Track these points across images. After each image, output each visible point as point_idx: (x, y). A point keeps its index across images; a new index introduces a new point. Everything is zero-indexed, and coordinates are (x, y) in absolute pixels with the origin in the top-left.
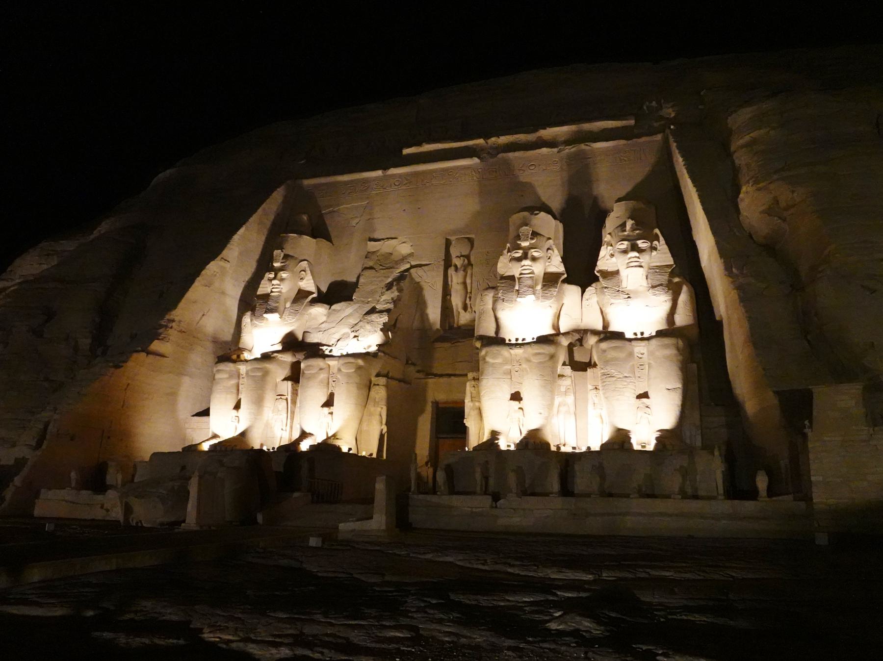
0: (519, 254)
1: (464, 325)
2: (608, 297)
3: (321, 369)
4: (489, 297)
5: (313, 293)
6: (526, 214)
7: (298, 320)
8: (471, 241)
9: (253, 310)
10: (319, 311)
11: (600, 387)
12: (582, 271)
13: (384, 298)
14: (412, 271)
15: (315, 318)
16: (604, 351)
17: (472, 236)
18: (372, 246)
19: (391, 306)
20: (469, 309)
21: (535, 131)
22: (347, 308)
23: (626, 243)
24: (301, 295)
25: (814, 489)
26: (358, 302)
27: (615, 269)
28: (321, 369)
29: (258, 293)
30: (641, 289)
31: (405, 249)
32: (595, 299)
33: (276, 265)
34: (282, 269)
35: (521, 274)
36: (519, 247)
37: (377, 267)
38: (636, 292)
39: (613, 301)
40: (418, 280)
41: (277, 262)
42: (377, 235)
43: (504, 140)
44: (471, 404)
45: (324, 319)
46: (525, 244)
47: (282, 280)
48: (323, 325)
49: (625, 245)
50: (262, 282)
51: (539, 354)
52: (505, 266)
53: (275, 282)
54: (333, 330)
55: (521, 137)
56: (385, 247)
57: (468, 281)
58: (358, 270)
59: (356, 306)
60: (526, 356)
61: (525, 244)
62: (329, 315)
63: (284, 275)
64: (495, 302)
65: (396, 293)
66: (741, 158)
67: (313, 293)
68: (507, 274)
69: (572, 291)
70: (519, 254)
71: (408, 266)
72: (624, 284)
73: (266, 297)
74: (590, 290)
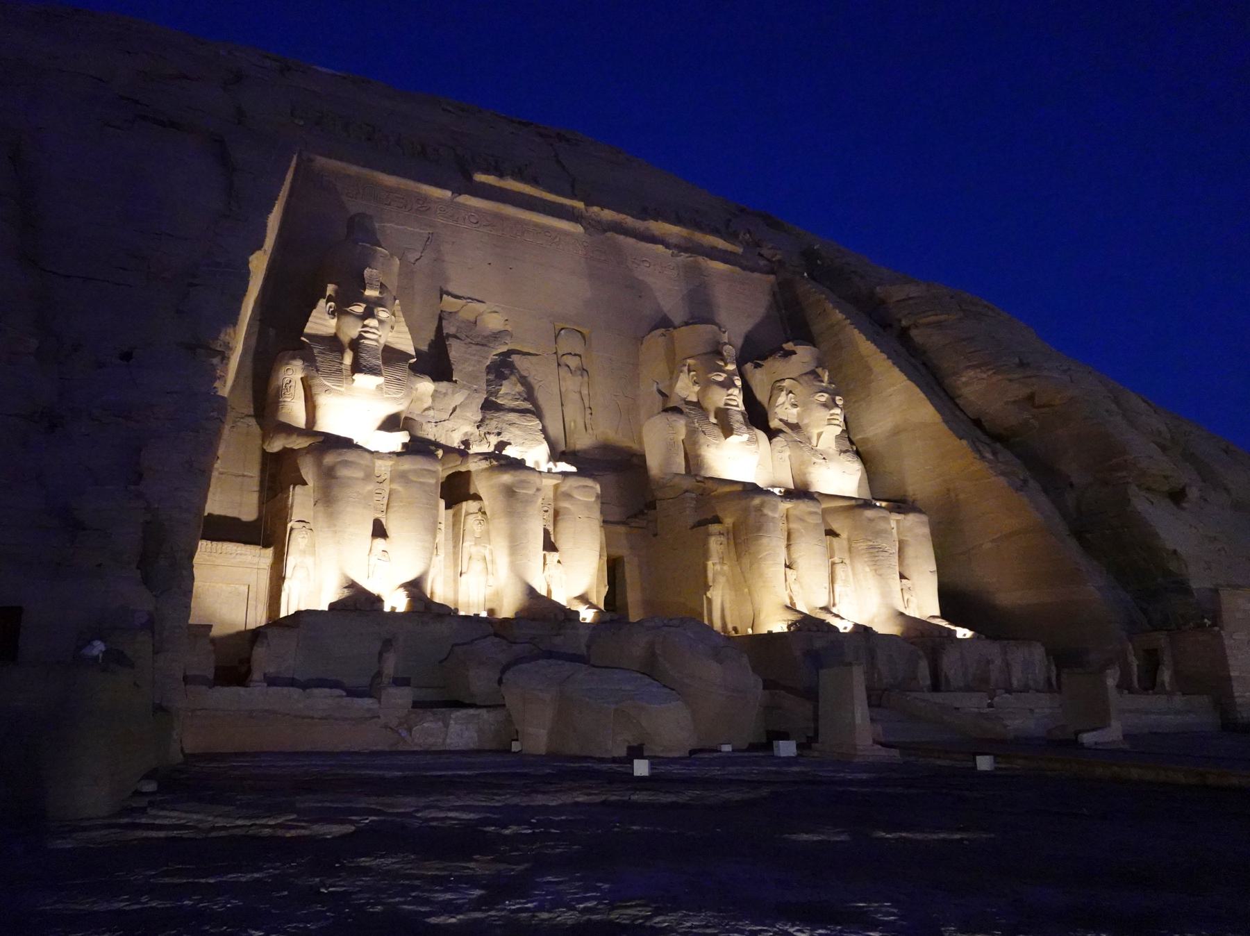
1: (585, 451)
2: (807, 454)
3: (538, 490)
4: (680, 427)
5: (412, 357)
7: (407, 395)
9: (310, 361)
10: (426, 386)
11: (847, 561)
12: (757, 417)
13: (503, 390)
14: (515, 358)
15: (419, 399)
16: (871, 520)
17: (584, 331)
19: (529, 406)
20: (590, 431)
22: (453, 393)
23: (826, 395)
24: (391, 356)
25: (1235, 684)
26: (463, 387)
27: (795, 421)
28: (538, 490)
29: (307, 330)
30: (831, 451)
31: (494, 322)
32: (787, 453)
33: (368, 293)
34: (379, 302)
35: (727, 404)
37: (463, 337)
38: (828, 454)
39: (814, 460)
40: (525, 374)
41: (372, 288)
42: (450, 290)
44: (718, 567)
45: (428, 402)
47: (381, 322)
48: (431, 413)
49: (824, 397)
50: (314, 313)
51: (816, 513)
52: (686, 388)
53: (372, 322)
54: (448, 425)
56: (468, 311)
57: (585, 392)
58: (429, 335)
59: (466, 392)
60: (796, 512)
62: (435, 395)
63: (383, 314)
64: (692, 433)
65: (520, 388)
67: (412, 357)
68: (689, 399)
69: (762, 435)
71: (504, 349)
72: (814, 442)
73: (333, 344)
74: (779, 440)
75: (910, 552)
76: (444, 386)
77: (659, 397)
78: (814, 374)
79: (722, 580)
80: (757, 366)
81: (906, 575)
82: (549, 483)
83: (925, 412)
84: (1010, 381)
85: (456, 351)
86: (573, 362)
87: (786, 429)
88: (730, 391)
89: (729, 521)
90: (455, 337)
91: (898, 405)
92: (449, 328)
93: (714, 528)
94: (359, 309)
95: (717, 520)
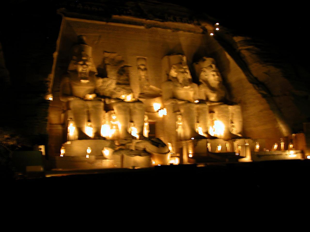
0: (182, 70)
6: (180, 56)
8: (145, 59)
12: (196, 80)
18: (107, 55)
21: (162, 21)
33: (84, 58)
34: (86, 61)
36: (182, 68)
43: (153, 22)
46: (185, 67)
52: (173, 73)
55: (159, 23)
61: (185, 67)
63: (88, 63)
66: (245, 53)
69: (195, 85)
70: (182, 70)
71: (122, 65)
75: (235, 116)
76: (105, 79)
77: (166, 76)
78: (211, 66)
79: (180, 127)
80: (197, 64)
81: (234, 121)
82: (131, 105)
83: (242, 76)
84: (263, 66)
85: (109, 69)
86: (142, 67)
87: (203, 83)
88: (184, 74)
89: (182, 111)
90: (109, 64)
91: (236, 74)
92: (107, 62)
93: (178, 113)
94: (81, 63)
95: (179, 111)
